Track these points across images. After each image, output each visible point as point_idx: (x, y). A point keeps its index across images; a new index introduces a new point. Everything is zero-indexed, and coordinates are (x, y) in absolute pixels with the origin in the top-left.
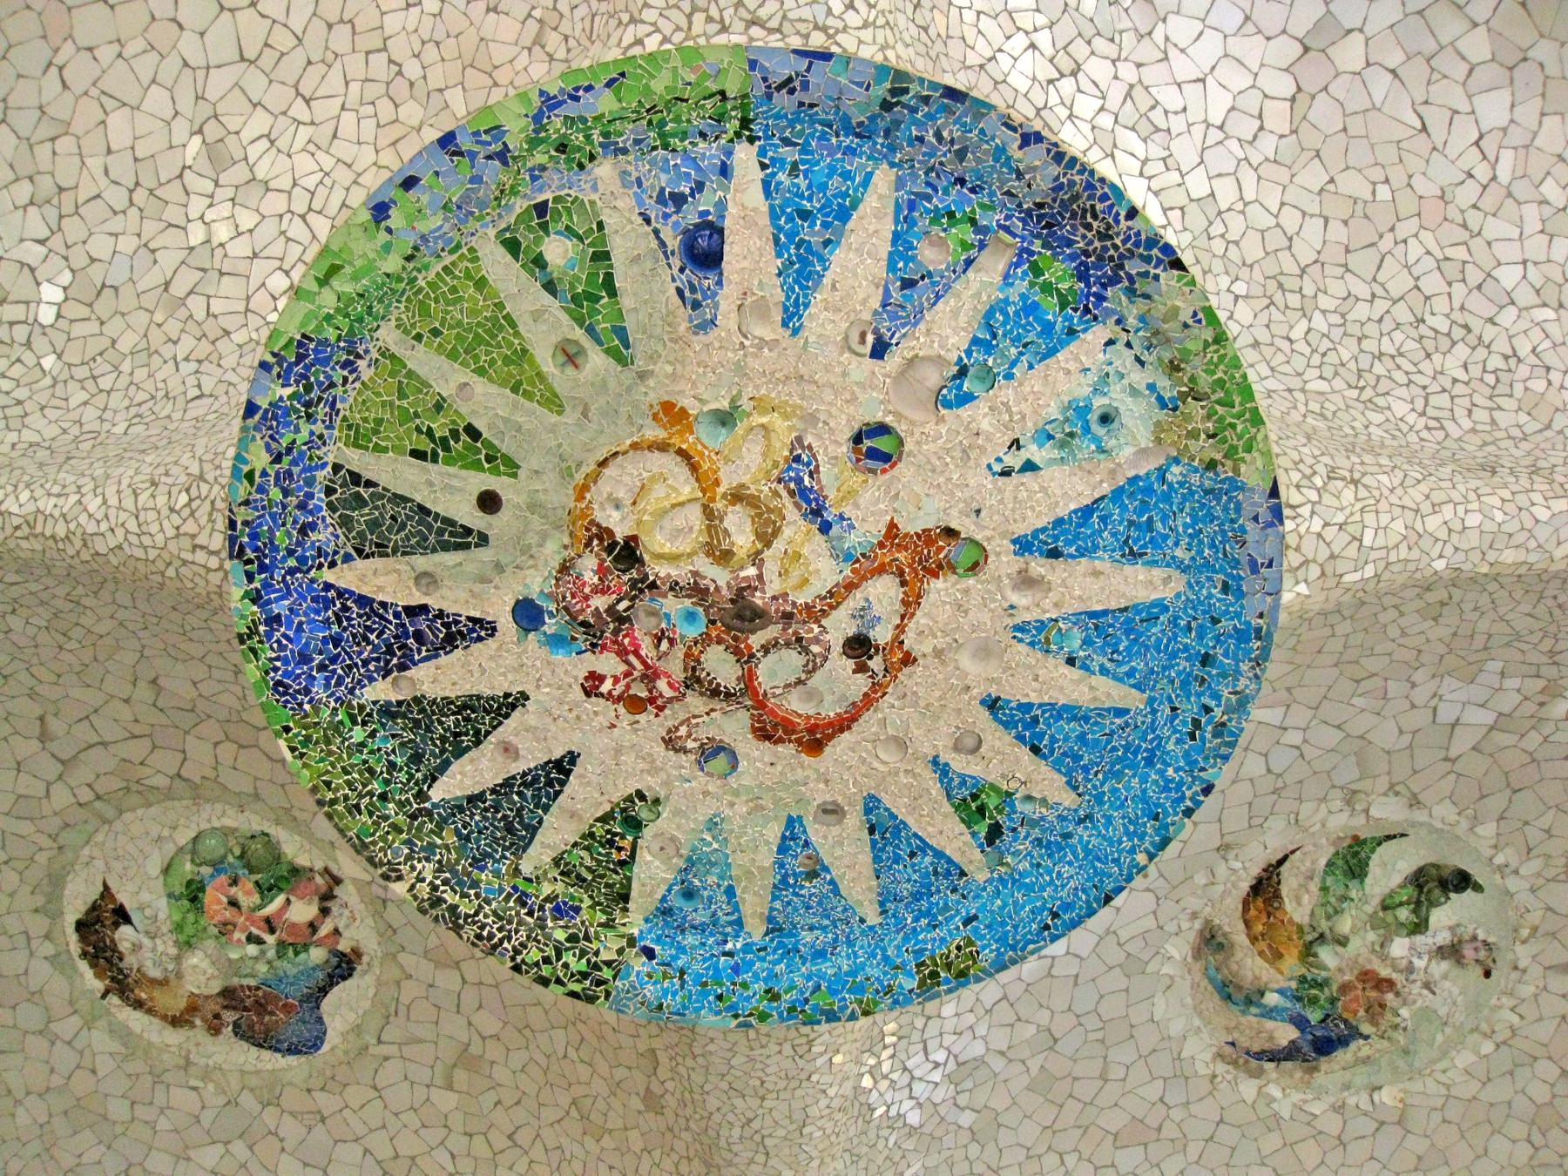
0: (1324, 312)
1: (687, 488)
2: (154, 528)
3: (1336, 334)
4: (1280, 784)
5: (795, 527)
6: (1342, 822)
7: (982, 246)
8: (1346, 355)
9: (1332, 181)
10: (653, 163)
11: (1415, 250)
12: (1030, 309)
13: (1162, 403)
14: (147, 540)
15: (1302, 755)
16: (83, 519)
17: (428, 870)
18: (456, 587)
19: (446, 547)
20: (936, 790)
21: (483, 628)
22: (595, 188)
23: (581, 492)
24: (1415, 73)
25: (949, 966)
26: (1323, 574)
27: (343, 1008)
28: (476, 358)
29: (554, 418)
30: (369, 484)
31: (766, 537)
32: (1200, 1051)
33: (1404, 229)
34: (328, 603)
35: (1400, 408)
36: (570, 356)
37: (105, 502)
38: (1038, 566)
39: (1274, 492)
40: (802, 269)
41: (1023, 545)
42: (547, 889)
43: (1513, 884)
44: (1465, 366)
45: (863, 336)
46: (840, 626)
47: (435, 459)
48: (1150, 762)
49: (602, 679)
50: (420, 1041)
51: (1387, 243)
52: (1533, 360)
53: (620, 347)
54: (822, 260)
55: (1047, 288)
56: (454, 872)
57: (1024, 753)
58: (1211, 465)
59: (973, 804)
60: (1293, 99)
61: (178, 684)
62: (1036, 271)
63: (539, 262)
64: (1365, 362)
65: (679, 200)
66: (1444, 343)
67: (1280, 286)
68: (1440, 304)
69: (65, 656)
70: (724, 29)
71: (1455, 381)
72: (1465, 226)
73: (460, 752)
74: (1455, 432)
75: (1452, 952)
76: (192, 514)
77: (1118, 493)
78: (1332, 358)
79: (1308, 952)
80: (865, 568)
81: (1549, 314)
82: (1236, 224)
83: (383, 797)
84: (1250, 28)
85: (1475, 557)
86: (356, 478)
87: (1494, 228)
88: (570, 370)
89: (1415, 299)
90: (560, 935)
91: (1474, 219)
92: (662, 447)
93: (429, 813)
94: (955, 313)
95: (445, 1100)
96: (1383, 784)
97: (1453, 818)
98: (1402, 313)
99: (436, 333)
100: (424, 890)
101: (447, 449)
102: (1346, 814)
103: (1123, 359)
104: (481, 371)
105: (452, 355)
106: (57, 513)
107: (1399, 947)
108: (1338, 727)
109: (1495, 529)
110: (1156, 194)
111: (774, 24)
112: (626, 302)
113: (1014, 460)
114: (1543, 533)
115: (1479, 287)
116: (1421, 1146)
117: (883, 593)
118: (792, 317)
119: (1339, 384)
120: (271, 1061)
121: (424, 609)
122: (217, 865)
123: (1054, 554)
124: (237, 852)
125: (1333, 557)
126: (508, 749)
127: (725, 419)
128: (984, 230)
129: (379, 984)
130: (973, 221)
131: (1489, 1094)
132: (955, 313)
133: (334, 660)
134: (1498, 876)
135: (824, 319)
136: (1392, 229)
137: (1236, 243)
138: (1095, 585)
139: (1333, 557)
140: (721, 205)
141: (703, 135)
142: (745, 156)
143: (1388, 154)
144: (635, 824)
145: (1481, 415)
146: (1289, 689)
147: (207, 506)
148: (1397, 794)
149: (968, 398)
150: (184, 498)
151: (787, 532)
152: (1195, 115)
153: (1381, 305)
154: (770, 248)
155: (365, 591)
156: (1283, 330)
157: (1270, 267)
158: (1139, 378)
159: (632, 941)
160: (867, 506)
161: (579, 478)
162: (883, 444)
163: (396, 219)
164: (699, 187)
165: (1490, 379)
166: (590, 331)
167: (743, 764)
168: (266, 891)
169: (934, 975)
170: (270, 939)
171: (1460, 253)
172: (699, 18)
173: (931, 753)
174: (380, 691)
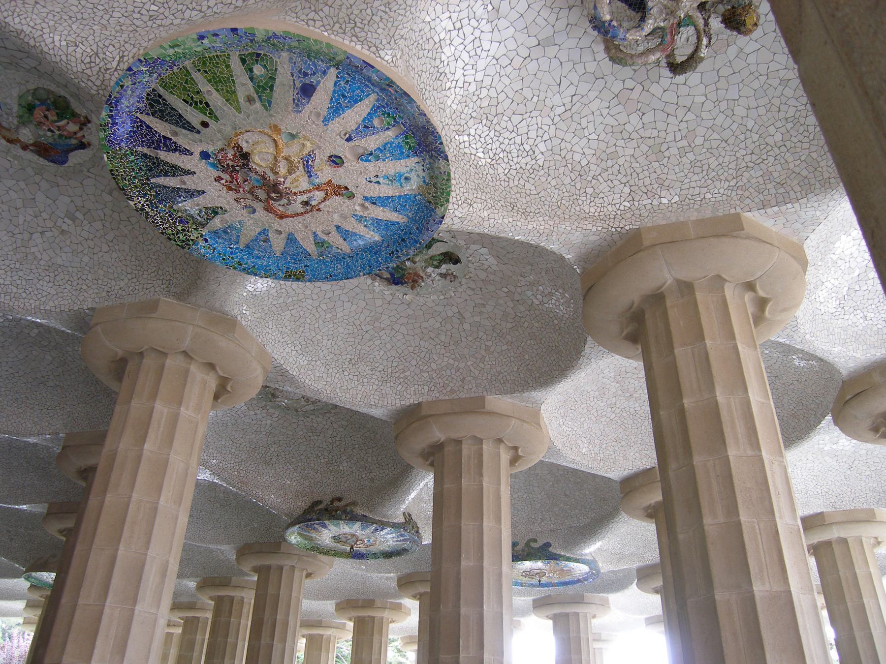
1: (272, 150)
2: (73, 64)
3: (495, 139)
5: (301, 171)
7: (394, 126)
8: (494, 147)
10: (302, 60)
11: (534, 121)
12: (399, 146)
13: (424, 181)
14: (69, 67)
16: (43, 44)
17: (143, 200)
18: (183, 139)
19: (185, 128)
20: (312, 239)
21: (187, 152)
22: (279, 58)
23: (237, 135)
24: (568, 66)
25: (295, 275)
27: (76, 157)
28: (217, 86)
29: (237, 114)
30: (164, 100)
31: (290, 172)
33: (534, 114)
34: (135, 122)
35: (500, 171)
36: (250, 100)
37: (53, 42)
38: (367, 204)
39: (443, 218)
40: (336, 110)
41: (366, 199)
42: (180, 214)
45: (345, 135)
46: (304, 198)
47: (191, 105)
48: (375, 253)
49: (222, 179)
51: (526, 116)
53: (268, 105)
54: (343, 110)
55: (407, 143)
56: (151, 203)
57: (341, 240)
58: (430, 202)
59: (319, 243)
62: (406, 138)
63: (251, 70)
64: (499, 150)
65: (306, 74)
66: (525, 154)
68: (531, 142)
70: (344, 33)
73: (166, 175)
74: (511, 185)
75: (444, 276)
76: (91, 68)
77: (400, 197)
78: (489, 147)
80: (318, 188)
81: (559, 158)
82: (484, 92)
83: (135, 177)
86: (160, 96)
87: (562, 125)
88: (248, 103)
90: (180, 228)
91: (557, 119)
92: (270, 136)
93: (148, 184)
94: (377, 140)
95: (108, 198)
98: (518, 140)
99: (206, 72)
100: (140, 206)
101: (196, 103)
103: (419, 168)
104: (218, 90)
105: (210, 81)
106: (31, 35)
107: (430, 270)
111: (361, 39)
112: (275, 95)
113: (373, 179)
116: (411, 312)
117: (319, 195)
118: (326, 121)
119: (487, 156)
121: (170, 139)
122: (43, 102)
123: (374, 203)
124: (52, 100)
127: (293, 136)
128: (397, 122)
130: (395, 119)
131: (437, 308)
132: (377, 140)
133: (131, 137)
135: (338, 125)
138: (382, 214)
140: (318, 82)
141: (322, 61)
142: (333, 71)
143: (543, 87)
144: (216, 213)
145: (522, 182)
147: (97, 68)
149: (370, 161)
150: (88, 60)
151: (298, 173)
152: (491, 53)
154: (328, 101)
155: (151, 126)
156: (479, 132)
157: (487, 110)
158: (421, 173)
159: (202, 236)
160: (325, 173)
161: (238, 131)
162: (337, 160)
163: (206, 41)
164: (314, 74)
165: (531, 171)
166: (260, 97)
167: (257, 213)
168: (61, 117)
169: (290, 276)
171: (546, 128)
172: (337, 25)
173: (314, 230)
174: (145, 150)
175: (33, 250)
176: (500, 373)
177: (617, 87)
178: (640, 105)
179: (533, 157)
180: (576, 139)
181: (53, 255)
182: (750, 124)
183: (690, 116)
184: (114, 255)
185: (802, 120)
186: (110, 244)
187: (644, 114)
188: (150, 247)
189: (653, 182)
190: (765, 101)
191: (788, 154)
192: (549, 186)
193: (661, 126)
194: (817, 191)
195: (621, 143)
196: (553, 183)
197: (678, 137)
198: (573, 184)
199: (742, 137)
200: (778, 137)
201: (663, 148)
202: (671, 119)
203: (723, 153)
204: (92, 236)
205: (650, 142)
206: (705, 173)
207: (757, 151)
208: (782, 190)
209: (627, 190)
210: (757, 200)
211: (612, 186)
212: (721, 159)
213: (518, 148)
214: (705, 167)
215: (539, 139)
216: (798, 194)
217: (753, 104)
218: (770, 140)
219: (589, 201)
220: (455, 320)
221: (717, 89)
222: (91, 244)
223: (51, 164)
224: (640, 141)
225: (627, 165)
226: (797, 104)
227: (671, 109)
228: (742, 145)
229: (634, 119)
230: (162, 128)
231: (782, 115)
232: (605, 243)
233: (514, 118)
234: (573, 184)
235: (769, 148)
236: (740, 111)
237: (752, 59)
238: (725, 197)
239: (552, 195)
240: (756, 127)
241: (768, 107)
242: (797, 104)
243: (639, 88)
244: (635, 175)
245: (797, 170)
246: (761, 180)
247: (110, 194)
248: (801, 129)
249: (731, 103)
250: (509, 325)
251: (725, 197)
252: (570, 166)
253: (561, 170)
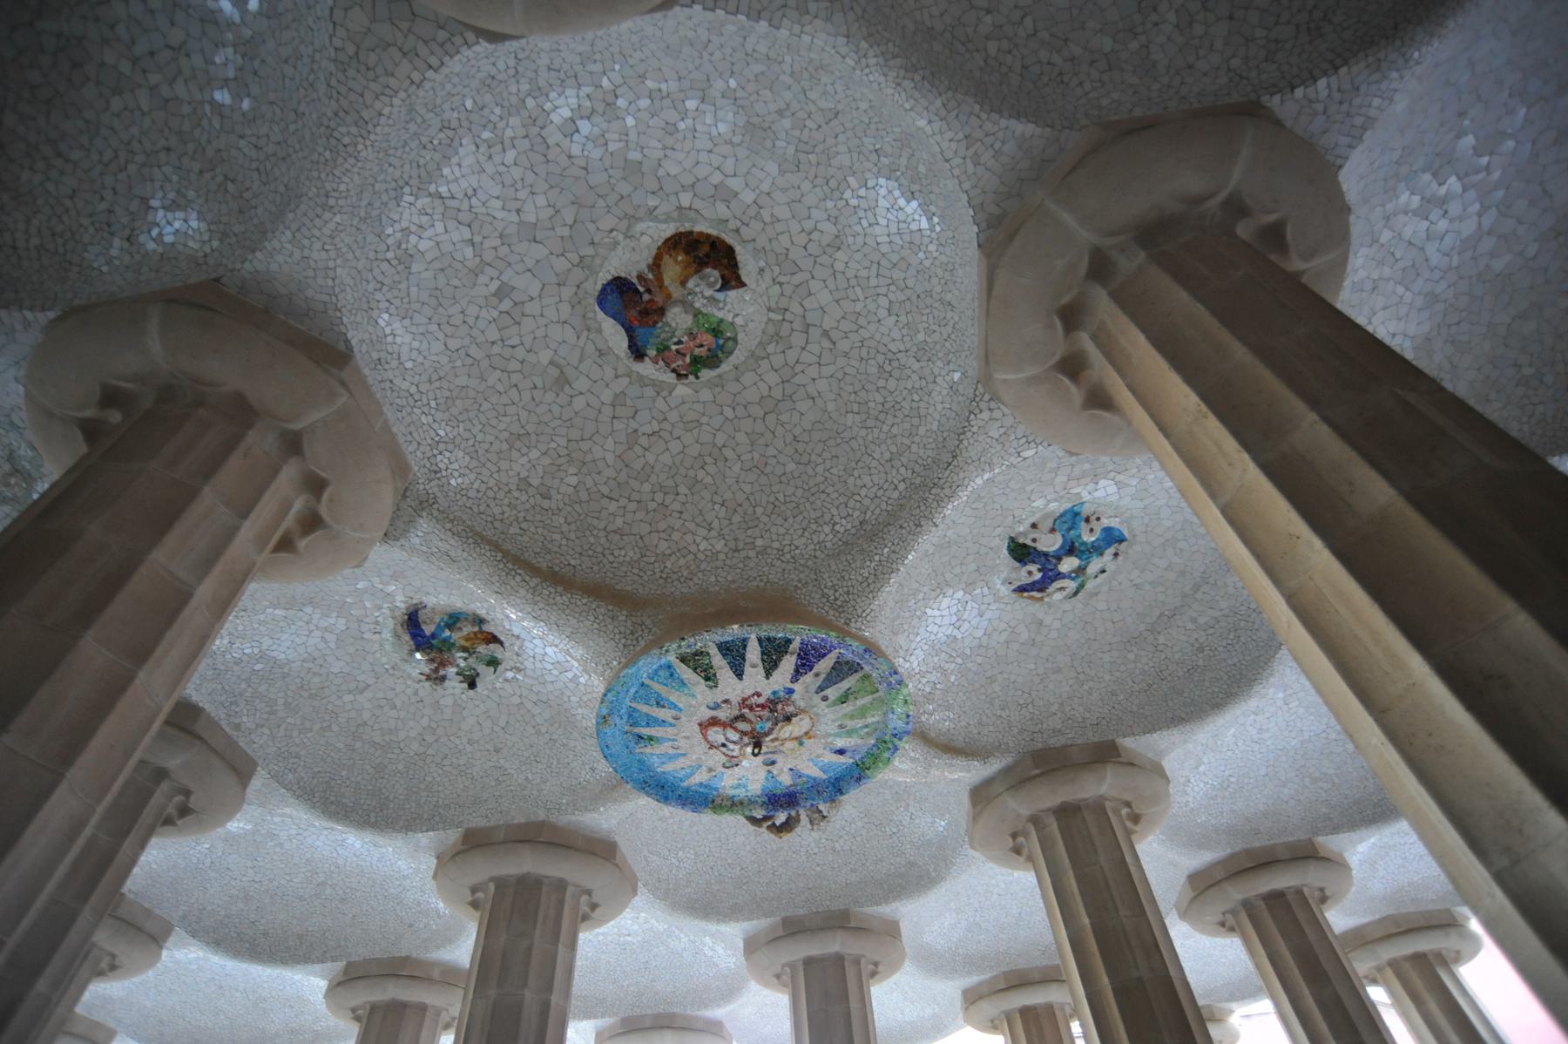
21: (795, 679)
27: (614, 335)
32: (431, 601)
50: (581, 361)
61: (803, 406)
69: (850, 389)
73: (763, 653)
79: (465, 649)
95: (545, 356)
120: (604, 277)
126: (754, 666)
129: (618, 358)
144: (707, 679)
170: (674, 348)
175: (439, 227)
176: (298, 757)
181: (429, 257)
184: (444, 360)
186: (462, 352)
188: (475, 421)
204: (471, 321)
220: (352, 686)
222: (457, 320)
223: (599, 287)
230: (824, 666)
247: (552, 363)
250: (378, 739)
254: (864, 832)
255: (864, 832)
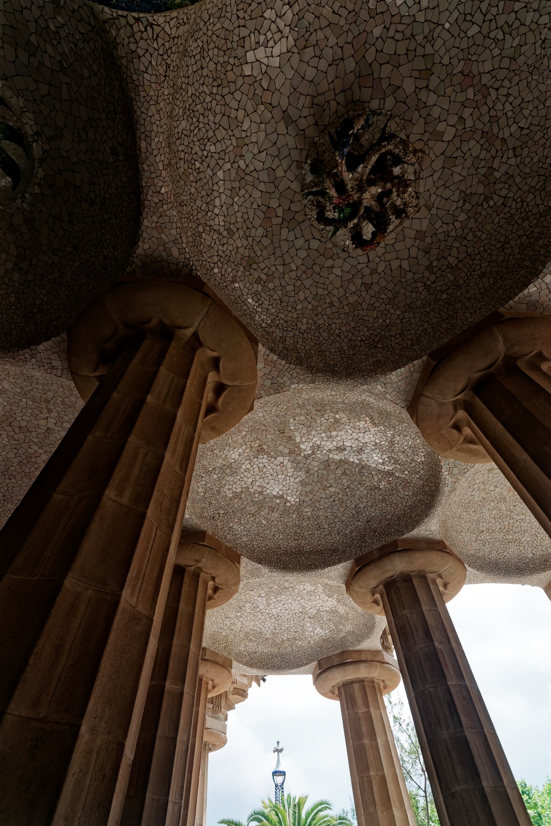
0: (211, 102)
4: (38, 102)
6: (29, 129)
9: (248, 115)
11: (228, 143)
15: (51, 111)
26: (133, 52)
43: (19, 201)
44: (196, 153)
51: (229, 131)
52: (198, 178)
60: (271, 104)
67: (219, 86)
68: (213, 148)
71: (192, 148)
72: (234, 162)
84: (292, 90)
85: (142, 130)
89: (214, 140)
91: (236, 166)
96: (47, 147)
97: (39, 176)
102: (31, 133)
108: (65, 125)
109: (153, 138)
110: (249, 35)
114: (151, 158)
115: (217, 164)
125: (140, 57)
134: (20, 196)
136: (234, 135)
137: (232, 70)
139: (140, 57)
146: (76, 99)
148: (43, 153)
153: (213, 125)
165: (193, 162)
171: (227, 160)
177: (274, 203)
178: (270, 229)
179: (203, 158)
180: (228, 193)
182: (299, 307)
183: (281, 268)
185: (321, 330)
187: (266, 236)
189: (231, 275)
190: (316, 304)
191: (300, 340)
192: (189, 187)
193: (265, 253)
194: (303, 367)
195: (241, 232)
196: (193, 190)
197: (265, 271)
198: (199, 210)
199: (290, 309)
200: (304, 327)
201: (255, 266)
202: (272, 258)
203: (274, 306)
205: (252, 255)
206: (257, 304)
207: (289, 323)
208: (286, 352)
209: (216, 259)
210: (270, 344)
211: (212, 246)
212: (270, 307)
213: (205, 137)
214: (260, 302)
215: (216, 156)
216: (293, 361)
217: (310, 299)
218: (299, 323)
219: (194, 232)
221: (304, 272)
224: (249, 246)
225: (230, 248)
226: (326, 320)
227: (278, 253)
228: (286, 313)
229: (261, 231)
231: (316, 319)
232: (173, 267)
233: (225, 118)
234: (199, 210)
235: (295, 328)
236: (301, 295)
237: (332, 277)
238: (255, 326)
239: (184, 194)
240: (300, 312)
241: (314, 308)
242: (326, 320)
243: (279, 220)
244: (227, 258)
245: (300, 350)
246: (278, 338)
248: (317, 334)
249: (302, 287)
251: (255, 326)
252: (209, 199)
253: (204, 193)
254: (472, 224)
255: (472, 224)
